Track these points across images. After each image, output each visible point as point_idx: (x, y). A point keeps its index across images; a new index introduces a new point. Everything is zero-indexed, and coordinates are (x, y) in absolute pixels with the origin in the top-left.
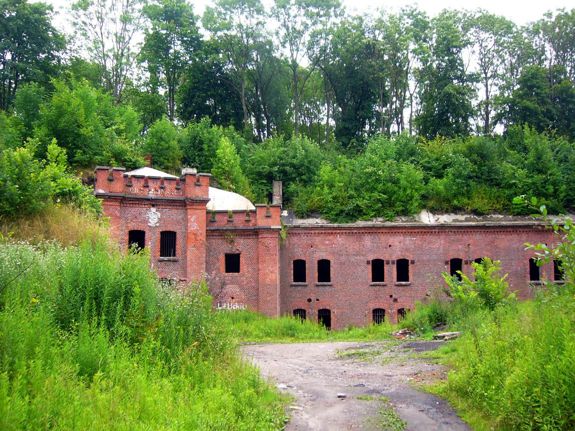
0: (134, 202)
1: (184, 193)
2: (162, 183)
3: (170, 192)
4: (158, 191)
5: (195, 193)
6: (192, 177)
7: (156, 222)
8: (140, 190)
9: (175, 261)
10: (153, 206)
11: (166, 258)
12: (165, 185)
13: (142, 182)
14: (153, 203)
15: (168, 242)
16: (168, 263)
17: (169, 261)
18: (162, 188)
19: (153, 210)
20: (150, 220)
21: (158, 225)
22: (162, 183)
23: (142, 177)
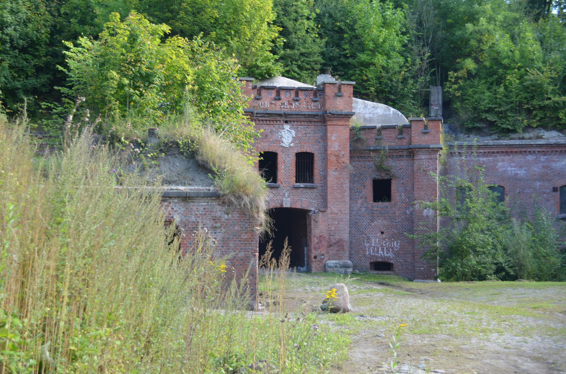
0: (263, 118)
1: (323, 105)
2: (297, 95)
3: (305, 106)
4: (292, 105)
5: (337, 105)
6: (332, 87)
7: (290, 141)
8: (271, 103)
9: (312, 188)
10: (286, 122)
11: (302, 185)
12: (300, 97)
13: (274, 94)
14: (287, 118)
15: (305, 164)
16: (305, 191)
17: (306, 188)
18: (297, 101)
19: (287, 127)
20: (284, 140)
21: (292, 145)
22: (297, 95)
23: (273, 88)
